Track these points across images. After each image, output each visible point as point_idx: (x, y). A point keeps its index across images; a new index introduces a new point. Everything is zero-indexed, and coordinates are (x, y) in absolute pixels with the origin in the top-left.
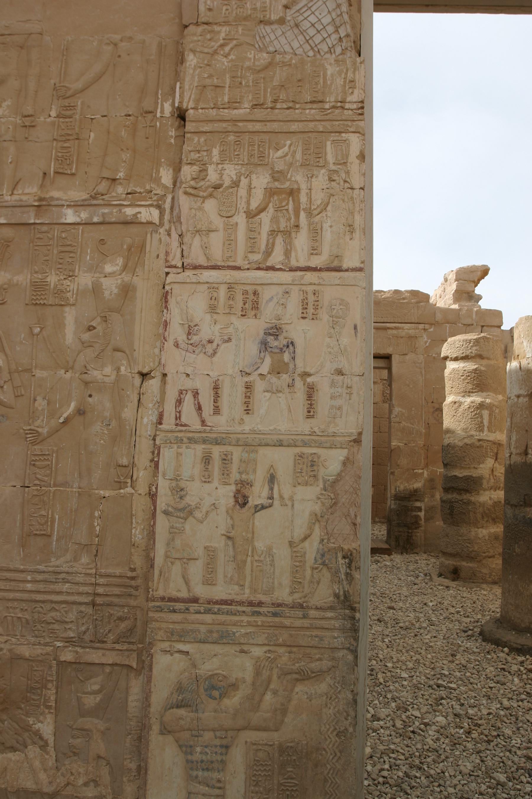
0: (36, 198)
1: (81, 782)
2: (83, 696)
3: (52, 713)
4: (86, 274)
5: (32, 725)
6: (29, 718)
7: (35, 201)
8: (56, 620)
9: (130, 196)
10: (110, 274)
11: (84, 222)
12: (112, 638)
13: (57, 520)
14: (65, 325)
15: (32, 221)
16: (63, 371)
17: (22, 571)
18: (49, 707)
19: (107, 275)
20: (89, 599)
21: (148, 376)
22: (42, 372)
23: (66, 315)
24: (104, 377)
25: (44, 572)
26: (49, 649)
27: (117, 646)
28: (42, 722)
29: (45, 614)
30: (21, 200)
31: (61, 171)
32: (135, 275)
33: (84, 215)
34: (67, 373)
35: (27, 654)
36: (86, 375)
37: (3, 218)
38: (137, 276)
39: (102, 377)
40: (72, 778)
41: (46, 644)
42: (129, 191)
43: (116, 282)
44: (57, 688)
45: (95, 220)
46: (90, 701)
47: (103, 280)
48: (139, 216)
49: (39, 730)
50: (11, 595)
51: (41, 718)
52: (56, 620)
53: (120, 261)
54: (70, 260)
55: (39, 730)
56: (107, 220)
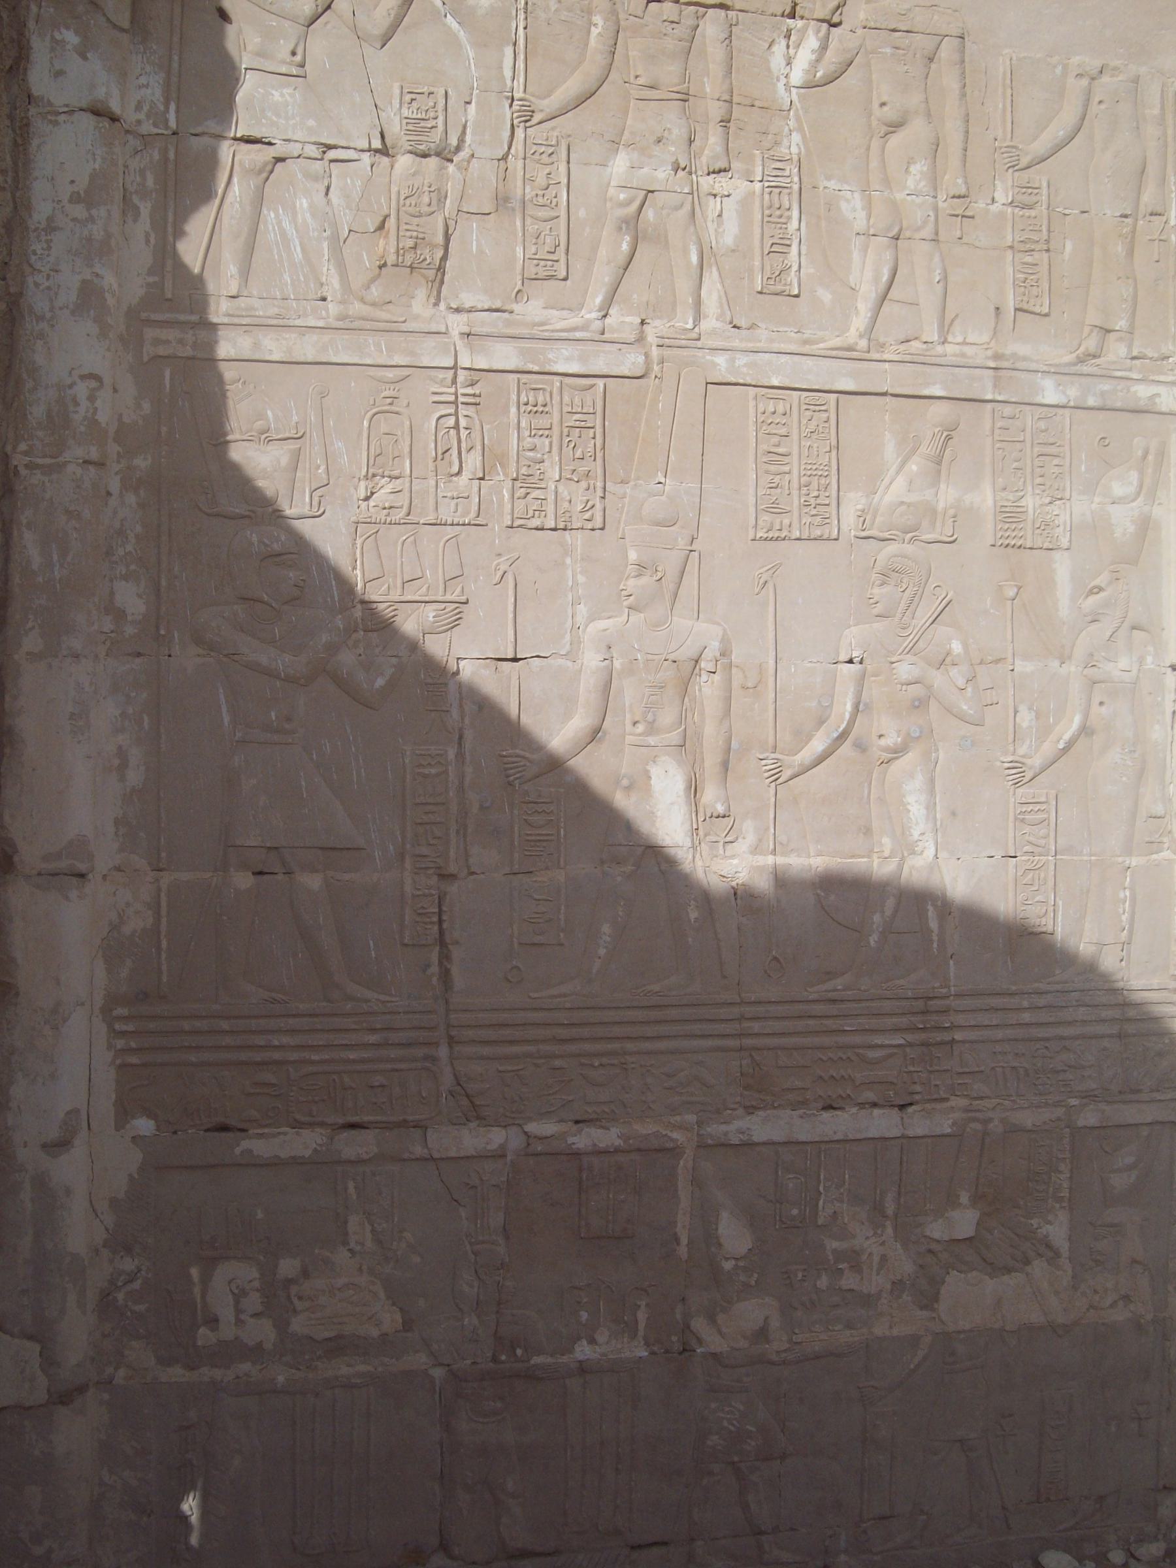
0: (990, 353)
1: (1109, 1301)
2: (1112, 1176)
3: (1064, 1207)
5: (1037, 1229)
6: (1032, 1219)
7: (988, 358)
8: (1069, 1066)
9: (1137, 362)
10: (1120, 498)
11: (1072, 404)
12: (1149, 1084)
13: (1061, 908)
15: (989, 397)
16: (1056, 663)
17: (1012, 994)
18: (1061, 1200)
20: (1115, 1030)
25: (1046, 993)
26: (1060, 1112)
27: (1158, 1096)
28: (1050, 1223)
29: (1051, 1058)
30: (963, 355)
31: (1025, 307)
32: (1157, 503)
33: (1073, 393)
35: (1029, 1124)
36: (1095, 669)
37: (938, 386)
38: (1159, 504)
40: (1097, 1298)
41: (1057, 1104)
42: (1135, 353)
44: (1071, 1171)
45: (1091, 401)
46: (1120, 1182)
47: (1112, 509)
48: (1157, 400)
49: (1046, 1236)
50: (999, 1034)
51: (1050, 1217)
52: (1069, 1066)
53: (1134, 476)
54: (1056, 470)
55: (1046, 1236)
56: (1109, 404)
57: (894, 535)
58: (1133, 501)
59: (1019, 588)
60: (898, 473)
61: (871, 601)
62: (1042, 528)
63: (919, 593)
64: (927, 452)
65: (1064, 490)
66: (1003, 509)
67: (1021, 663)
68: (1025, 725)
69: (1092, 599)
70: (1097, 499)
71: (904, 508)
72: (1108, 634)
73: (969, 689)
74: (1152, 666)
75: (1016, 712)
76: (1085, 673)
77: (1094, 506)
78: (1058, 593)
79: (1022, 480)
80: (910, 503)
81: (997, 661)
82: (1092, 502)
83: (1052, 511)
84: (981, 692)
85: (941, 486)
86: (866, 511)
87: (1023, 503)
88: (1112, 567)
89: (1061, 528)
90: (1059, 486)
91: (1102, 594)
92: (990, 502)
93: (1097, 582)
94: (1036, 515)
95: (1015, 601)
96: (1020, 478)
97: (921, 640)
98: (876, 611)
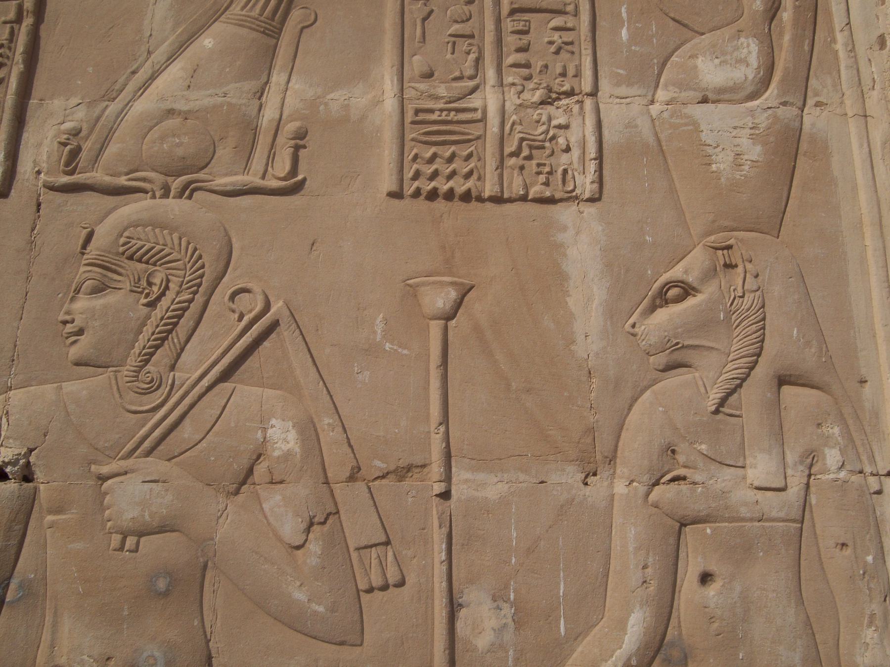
4: (623, 90)
10: (721, 91)
14: (562, 277)
16: (572, 475)
19: (711, 96)
22: (481, 476)
23: (565, 237)
24: (760, 495)
32: (810, 102)
34: (591, 480)
36: (683, 487)
38: (818, 104)
47: (699, 111)
57: (144, 180)
59: (465, 292)
60: (172, 58)
61: (69, 328)
62: (525, 152)
63: (195, 308)
64: (244, 13)
65: (578, 75)
66: (421, 117)
67: (468, 475)
68: (483, 642)
69: (662, 315)
70: (662, 95)
71: (171, 123)
72: (715, 396)
73: (314, 547)
74: (842, 474)
75: (453, 608)
76: (653, 497)
77: (655, 109)
78: (571, 301)
79: (472, 56)
80: (189, 112)
81: (403, 472)
82: (652, 102)
83: (550, 119)
84: (354, 555)
85: (274, 78)
86: (82, 135)
87: (475, 101)
88: (712, 238)
89: (575, 153)
90: (565, 67)
91: (690, 302)
92: (390, 104)
93: (677, 272)
95: (453, 323)
96: (468, 53)
97: (187, 421)
98: (74, 352)
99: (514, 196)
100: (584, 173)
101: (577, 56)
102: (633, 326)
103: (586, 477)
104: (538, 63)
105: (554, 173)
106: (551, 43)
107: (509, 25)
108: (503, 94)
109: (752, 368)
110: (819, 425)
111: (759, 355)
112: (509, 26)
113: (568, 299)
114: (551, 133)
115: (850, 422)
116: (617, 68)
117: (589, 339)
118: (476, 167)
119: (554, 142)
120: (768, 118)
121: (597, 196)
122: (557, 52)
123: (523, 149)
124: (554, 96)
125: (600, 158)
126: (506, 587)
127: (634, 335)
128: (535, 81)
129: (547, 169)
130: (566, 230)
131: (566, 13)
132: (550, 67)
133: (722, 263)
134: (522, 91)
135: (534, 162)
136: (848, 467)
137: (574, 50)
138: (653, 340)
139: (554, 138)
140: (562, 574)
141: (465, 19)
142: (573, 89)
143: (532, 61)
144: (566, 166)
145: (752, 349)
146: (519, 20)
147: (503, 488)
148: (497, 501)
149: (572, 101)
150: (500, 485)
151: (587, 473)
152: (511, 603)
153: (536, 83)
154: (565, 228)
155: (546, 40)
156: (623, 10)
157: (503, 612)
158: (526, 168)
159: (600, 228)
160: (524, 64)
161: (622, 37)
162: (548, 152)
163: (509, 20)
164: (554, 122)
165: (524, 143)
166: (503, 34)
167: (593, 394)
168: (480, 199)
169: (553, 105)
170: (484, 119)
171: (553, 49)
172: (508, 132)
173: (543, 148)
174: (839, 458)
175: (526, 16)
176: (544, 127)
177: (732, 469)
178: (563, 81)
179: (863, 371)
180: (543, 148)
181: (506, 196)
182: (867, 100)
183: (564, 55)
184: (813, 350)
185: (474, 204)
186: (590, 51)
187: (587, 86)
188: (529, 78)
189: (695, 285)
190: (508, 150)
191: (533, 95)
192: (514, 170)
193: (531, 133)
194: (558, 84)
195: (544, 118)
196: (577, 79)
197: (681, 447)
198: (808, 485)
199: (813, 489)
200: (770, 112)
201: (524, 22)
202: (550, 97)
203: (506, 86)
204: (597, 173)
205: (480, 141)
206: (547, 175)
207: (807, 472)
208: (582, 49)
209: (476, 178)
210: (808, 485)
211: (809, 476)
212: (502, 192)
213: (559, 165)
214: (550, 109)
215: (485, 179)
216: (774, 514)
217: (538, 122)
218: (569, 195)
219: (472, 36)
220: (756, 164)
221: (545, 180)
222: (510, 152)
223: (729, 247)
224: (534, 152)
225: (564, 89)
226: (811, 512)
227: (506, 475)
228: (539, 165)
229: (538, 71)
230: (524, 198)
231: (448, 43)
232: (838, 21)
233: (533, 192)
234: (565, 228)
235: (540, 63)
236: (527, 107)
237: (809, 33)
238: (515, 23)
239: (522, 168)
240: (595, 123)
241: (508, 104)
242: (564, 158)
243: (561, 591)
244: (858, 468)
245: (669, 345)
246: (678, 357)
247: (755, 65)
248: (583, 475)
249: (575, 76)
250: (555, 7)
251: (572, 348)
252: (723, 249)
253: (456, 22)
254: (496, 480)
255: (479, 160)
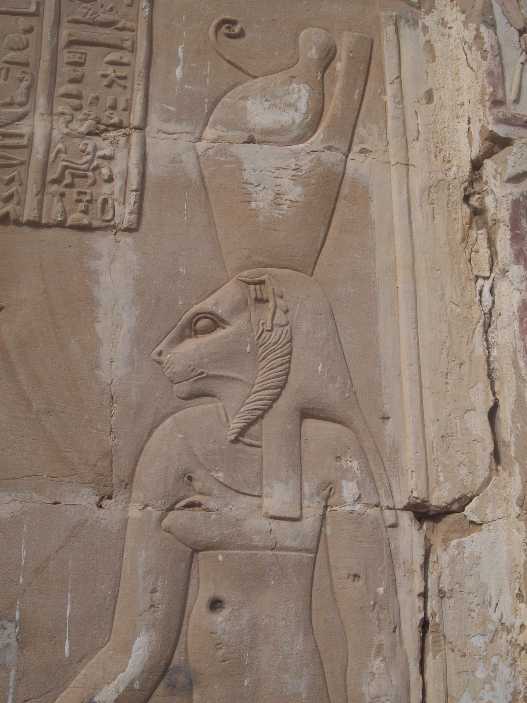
4: (171, 127)
19: (257, 137)
21: (450, 519)
23: (101, 264)
24: (274, 524)
32: (356, 148)
34: (106, 503)
36: (198, 513)
38: (363, 151)
39: (265, 524)
43: (292, 163)
58: (301, 139)
62: (68, 180)
65: (128, 109)
70: (209, 133)
72: (235, 425)
74: (358, 507)
76: (166, 522)
77: (201, 146)
78: (99, 327)
79: (25, 84)
82: (200, 139)
83: (95, 149)
87: (23, 128)
88: (246, 273)
89: (118, 184)
90: (115, 101)
91: (219, 333)
93: (207, 304)
94: (52, 155)
96: (21, 81)
99: (52, 222)
100: (124, 204)
101: (128, 91)
102: (160, 354)
103: (101, 500)
104: (90, 94)
105: (94, 202)
106: (105, 76)
107: (65, 56)
108: (52, 122)
109: (274, 400)
110: (338, 458)
111: (283, 387)
112: (65, 58)
113: (96, 325)
114: (95, 163)
115: (370, 457)
116: (168, 105)
117: (114, 365)
118: (17, 191)
119: (97, 172)
120: (311, 161)
121: (134, 226)
122: (109, 86)
123: (66, 177)
124: (102, 127)
125: (141, 189)
126: (13, 605)
127: (160, 363)
128: (85, 112)
129: (88, 198)
130: (101, 258)
131: (123, 49)
132: (101, 100)
133: (253, 297)
134: (70, 122)
135: (75, 190)
136: (365, 500)
137: (127, 84)
138: (177, 368)
139: (97, 168)
140: (69, 596)
141: (21, 47)
142: (121, 122)
143: (84, 93)
144: (107, 196)
145: (276, 382)
146: (76, 52)
147: (16, 507)
148: (8, 520)
149: (119, 134)
150: (13, 504)
151: (102, 495)
152: (16, 622)
153: (85, 114)
154: (100, 256)
155: (100, 73)
156: (180, 50)
157: (7, 632)
158: (67, 196)
159: (135, 258)
160: (75, 95)
161: (176, 75)
162: (90, 181)
163: (65, 51)
164: (100, 153)
165: (67, 171)
166: (58, 65)
167: (113, 419)
168: (17, 223)
169: (100, 136)
170: (30, 146)
171: (105, 82)
172: (52, 160)
173: (86, 177)
174: (356, 490)
175: (84, 49)
176: (89, 157)
177: (248, 498)
178: (112, 114)
179: (387, 408)
180: (86, 177)
181: (44, 221)
182: (410, 150)
183: (116, 89)
184: (337, 385)
185: (12, 228)
186: (142, 87)
187: (135, 120)
188: (78, 109)
189: (224, 316)
190: (50, 177)
191: (82, 126)
192: (54, 196)
193: (75, 161)
194: (107, 116)
195: (89, 148)
196: (127, 113)
197: (199, 474)
198: (323, 517)
199: (329, 521)
200: (314, 155)
201: (79, 55)
202: (97, 129)
203: (56, 114)
204: (137, 204)
205: (23, 168)
206: (86, 204)
207: (323, 504)
208: (135, 83)
209: (15, 202)
210: (323, 517)
211: (326, 507)
212: (40, 217)
213: (100, 195)
214: (98, 140)
215: (25, 204)
216: (287, 543)
217: (83, 151)
218: (107, 224)
219: (26, 64)
220: (295, 204)
221: (84, 208)
222: (52, 178)
223: (262, 283)
224: (76, 180)
225: (113, 121)
226: (326, 543)
227: (19, 495)
228: (79, 193)
229: (89, 102)
230: (61, 225)
231: (2, 69)
232: (390, 74)
233: (73, 218)
234: (100, 256)
235: (92, 95)
236: (74, 136)
237: (360, 83)
238: (71, 54)
239: (62, 195)
240: (139, 156)
241: (55, 133)
242: (106, 188)
243: (68, 612)
244: (375, 501)
245: (193, 374)
246: (201, 386)
247: (304, 110)
248: (98, 499)
249: (125, 110)
250: (112, 42)
251: (97, 372)
252: (255, 284)
253: (13, 49)
254: (9, 499)
255: (20, 185)
